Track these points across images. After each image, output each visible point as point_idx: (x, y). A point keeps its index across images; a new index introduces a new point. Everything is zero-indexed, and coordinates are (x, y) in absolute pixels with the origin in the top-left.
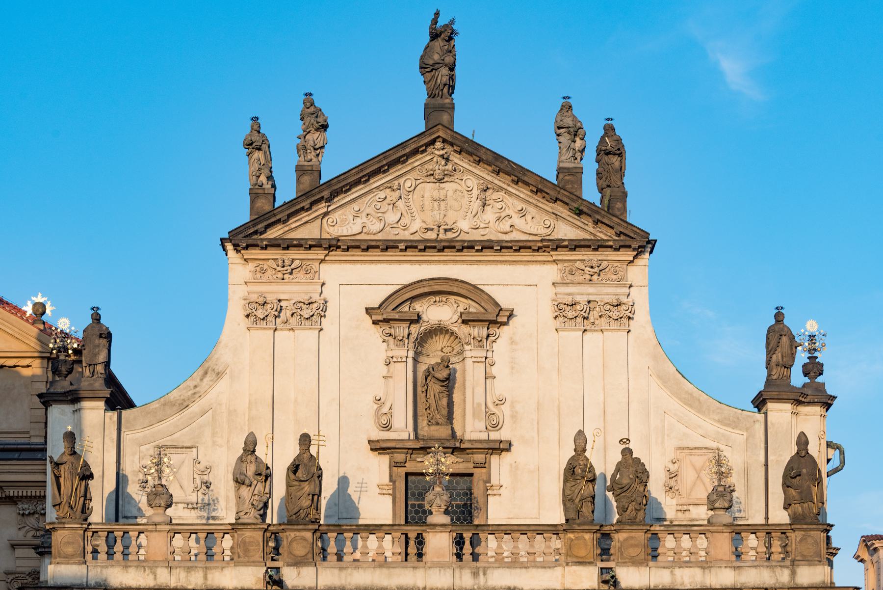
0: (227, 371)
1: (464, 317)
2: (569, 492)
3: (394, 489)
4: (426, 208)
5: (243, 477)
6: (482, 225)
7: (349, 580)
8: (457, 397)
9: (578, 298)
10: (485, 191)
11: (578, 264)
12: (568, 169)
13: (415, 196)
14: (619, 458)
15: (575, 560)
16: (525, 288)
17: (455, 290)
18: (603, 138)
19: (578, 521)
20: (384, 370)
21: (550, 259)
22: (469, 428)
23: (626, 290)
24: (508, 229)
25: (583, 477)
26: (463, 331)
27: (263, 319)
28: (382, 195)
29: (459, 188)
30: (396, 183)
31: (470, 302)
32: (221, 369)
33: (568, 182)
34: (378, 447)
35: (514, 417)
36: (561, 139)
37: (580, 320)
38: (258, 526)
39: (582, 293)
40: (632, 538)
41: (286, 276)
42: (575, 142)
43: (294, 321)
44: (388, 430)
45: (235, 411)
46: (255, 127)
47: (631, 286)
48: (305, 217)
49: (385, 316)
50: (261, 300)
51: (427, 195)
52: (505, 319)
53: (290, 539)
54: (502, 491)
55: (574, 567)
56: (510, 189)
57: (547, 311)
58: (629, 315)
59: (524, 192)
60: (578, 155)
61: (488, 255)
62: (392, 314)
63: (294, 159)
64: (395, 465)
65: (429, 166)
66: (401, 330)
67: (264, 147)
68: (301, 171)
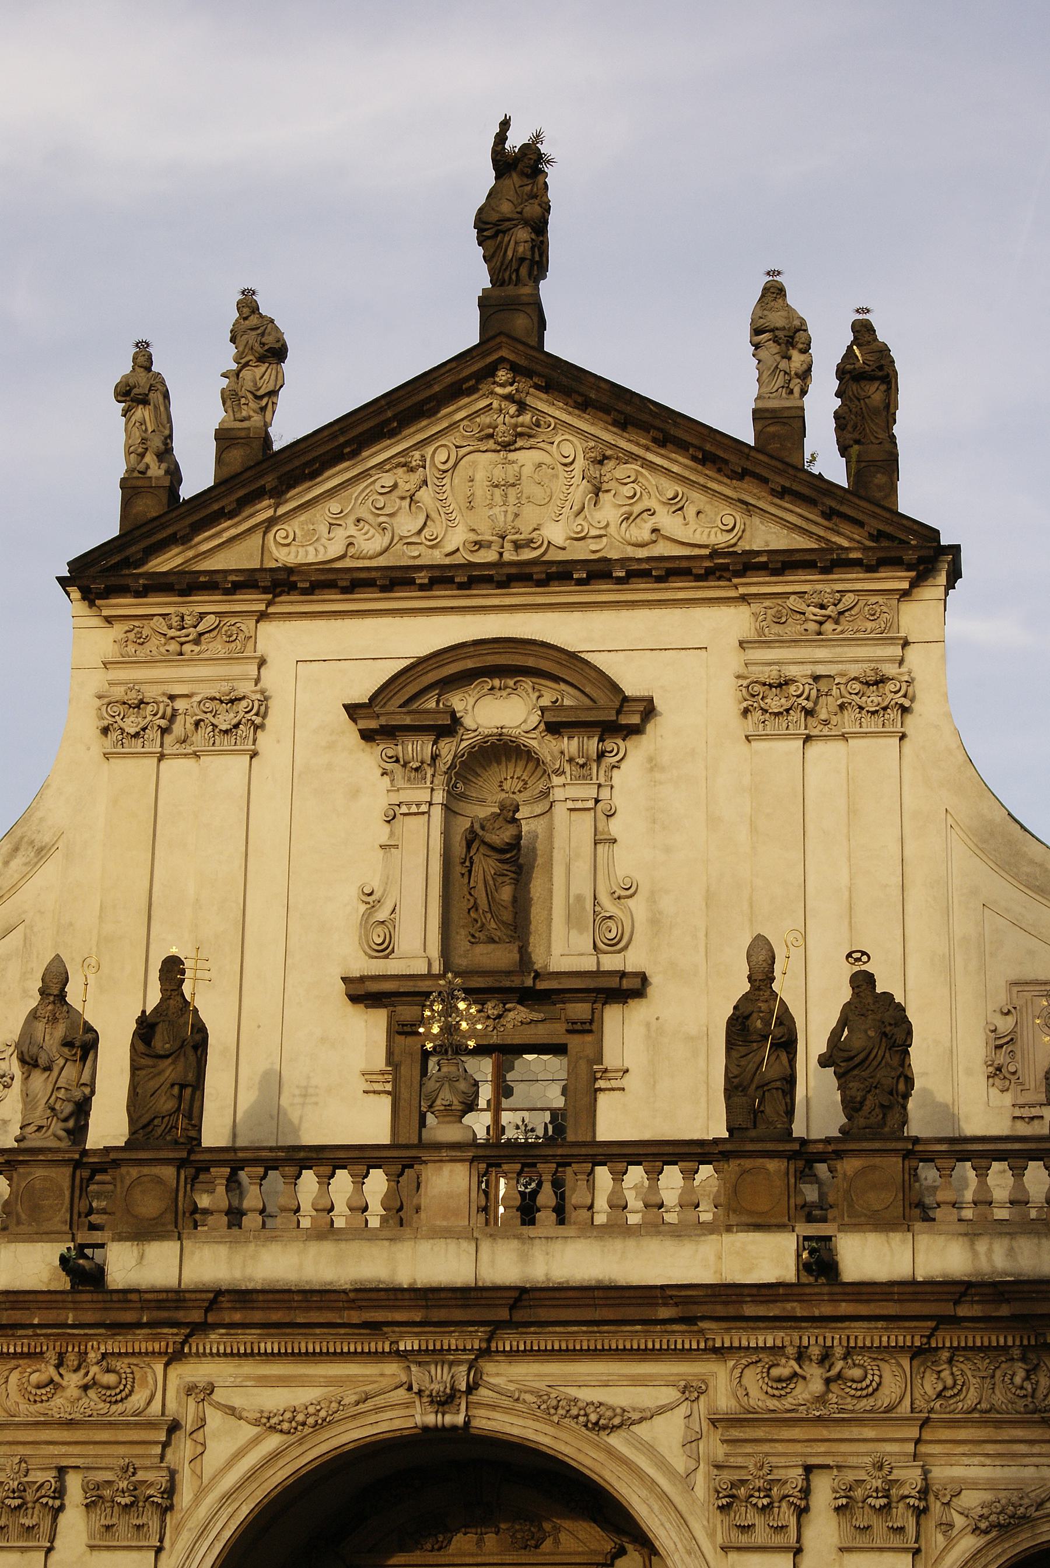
0: (60, 844)
1: (550, 717)
2: (736, 1071)
3: (395, 1082)
4: (478, 500)
5: (34, 1050)
6: (594, 532)
7: (249, 1271)
8: (537, 888)
9: (792, 671)
10: (601, 463)
11: (793, 602)
12: (773, 411)
13: (456, 481)
14: (846, 994)
15: (745, 1219)
16: (683, 657)
17: (531, 662)
18: (850, 348)
19: (753, 1133)
20: (382, 833)
21: (733, 593)
22: (558, 947)
23: (897, 651)
24: (646, 535)
25: (765, 1038)
26: (547, 747)
27: (136, 735)
28: (387, 480)
29: (546, 458)
30: (417, 454)
31: (563, 686)
32: (46, 838)
33: (774, 436)
34: (363, 993)
35: (655, 921)
36: (763, 353)
37: (796, 716)
38: (67, 1156)
39: (799, 661)
40: (874, 1168)
41: (187, 648)
42: (789, 358)
43: (199, 739)
44: (386, 957)
45: (71, 924)
46: (141, 360)
47: (906, 644)
48: (229, 529)
49: (383, 721)
50: (133, 697)
51: (480, 476)
52: (636, 719)
53: (128, 1182)
54: (626, 1082)
55: (742, 1236)
56: (650, 457)
57: (727, 699)
58: (901, 701)
59: (679, 463)
60: (796, 385)
61: (604, 592)
62: (396, 715)
63: (216, 415)
64: (401, 1030)
65: (485, 419)
66: (419, 748)
67: (155, 397)
68: (224, 438)
